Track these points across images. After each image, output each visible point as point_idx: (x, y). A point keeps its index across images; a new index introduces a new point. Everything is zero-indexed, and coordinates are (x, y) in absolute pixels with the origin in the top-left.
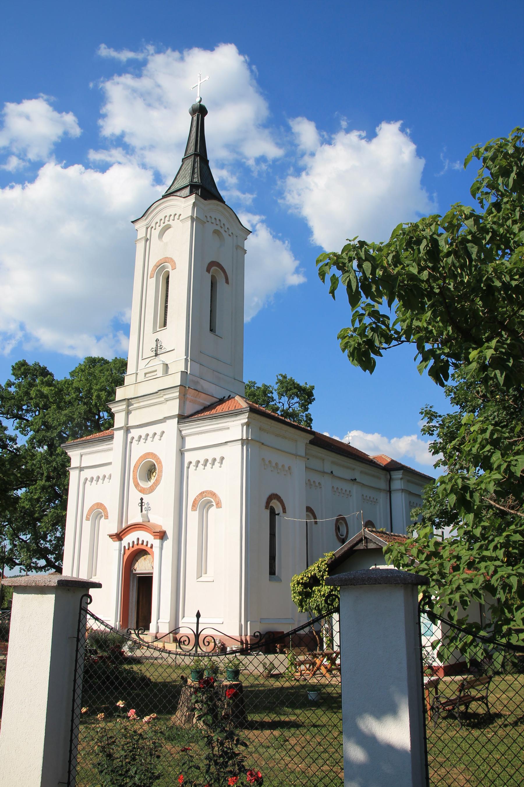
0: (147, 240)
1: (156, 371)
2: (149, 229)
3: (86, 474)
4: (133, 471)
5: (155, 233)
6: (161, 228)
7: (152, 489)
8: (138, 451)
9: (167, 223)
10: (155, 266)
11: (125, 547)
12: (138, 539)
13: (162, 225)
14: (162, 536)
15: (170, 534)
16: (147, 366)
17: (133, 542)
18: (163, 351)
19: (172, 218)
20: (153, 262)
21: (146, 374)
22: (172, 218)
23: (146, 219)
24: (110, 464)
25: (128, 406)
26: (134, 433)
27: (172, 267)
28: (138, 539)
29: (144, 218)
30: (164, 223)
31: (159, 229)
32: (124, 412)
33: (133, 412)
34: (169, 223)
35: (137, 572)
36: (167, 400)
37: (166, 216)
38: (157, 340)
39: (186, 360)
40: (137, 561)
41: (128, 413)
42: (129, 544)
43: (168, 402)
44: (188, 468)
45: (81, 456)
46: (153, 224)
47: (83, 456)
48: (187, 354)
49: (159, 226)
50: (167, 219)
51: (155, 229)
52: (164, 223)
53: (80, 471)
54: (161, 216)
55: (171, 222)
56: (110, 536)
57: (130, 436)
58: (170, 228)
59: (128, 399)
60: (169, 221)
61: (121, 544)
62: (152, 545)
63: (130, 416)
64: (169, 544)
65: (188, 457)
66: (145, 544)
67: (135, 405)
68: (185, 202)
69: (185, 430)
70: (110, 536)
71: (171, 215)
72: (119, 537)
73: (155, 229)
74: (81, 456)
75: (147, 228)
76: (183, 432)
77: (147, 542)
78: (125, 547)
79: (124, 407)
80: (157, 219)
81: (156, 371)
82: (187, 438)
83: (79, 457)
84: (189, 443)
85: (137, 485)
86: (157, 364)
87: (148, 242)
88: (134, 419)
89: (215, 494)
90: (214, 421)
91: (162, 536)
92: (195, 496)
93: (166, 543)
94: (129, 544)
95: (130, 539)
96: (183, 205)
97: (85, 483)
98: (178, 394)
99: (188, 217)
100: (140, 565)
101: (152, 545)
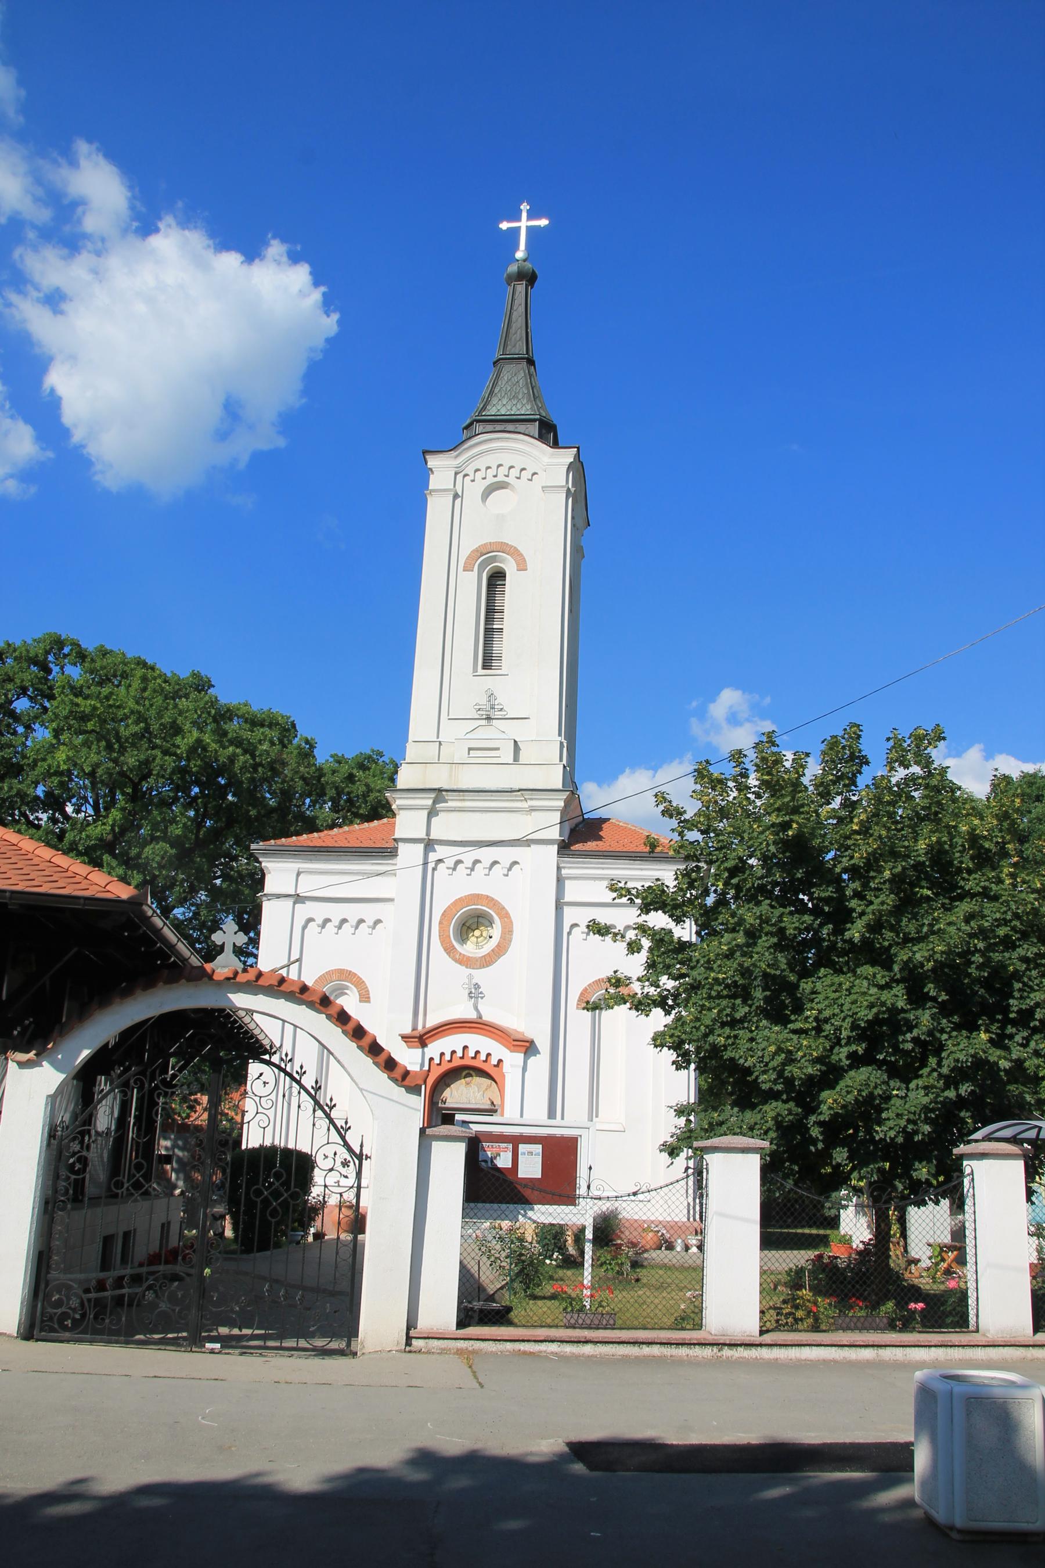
0: (456, 496)
1: (498, 749)
2: (460, 477)
3: (304, 911)
4: (440, 923)
5: (473, 490)
6: (487, 482)
7: (487, 961)
8: (451, 888)
9: (501, 478)
10: (476, 550)
11: (431, 1059)
12: (465, 1048)
13: (490, 480)
14: (529, 1048)
15: (543, 1044)
16: (468, 736)
17: (453, 1052)
18: (498, 715)
19: (514, 472)
20: (468, 545)
21: (470, 749)
22: (514, 472)
23: (456, 457)
24: (391, 900)
25: (435, 802)
26: (441, 851)
27: (518, 565)
28: (465, 1048)
29: (454, 454)
30: (495, 476)
31: (481, 486)
32: (425, 813)
33: (441, 814)
34: (506, 479)
35: (447, 1105)
36: (533, 809)
37: (500, 466)
39: (561, 743)
40: (449, 1086)
41: (432, 813)
42: (442, 1054)
43: (533, 813)
44: (569, 933)
45: (298, 874)
46: (470, 470)
47: (302, 876)
48: (560, 735)
49: (484, 478)
50: (502, 471)
51: (473, 481)
52: (495, 476)
53: (295, 903)
54: (492, 460)
55: (511, 480)
57: (433, 857)
58: (503, 488)
59: (440, 790)
60: (507, 476)
61: (423, 1054)
63: (434, 820)
64: (540, 1064)
65: (570, 915)
66: (483, 1057)
67: (450, 804)
68: (552, 455)
69: (570, 868)
70: (405, 1038)
73: (473, 481)
74: (298, 874)
75: (456, 474)
76: (564, 872)
77: (489, 1055)
78: (431, 1059)
79: (430, 802)
80: (481, 463)
81: (498, 749)
82: (567, 882)
83: (295, 875)
84: (573, 892)
85: (450, 950)
86: (487, 734)
87: (458, 501)
88: (444, 827)
90: (637, 865)
91: (529, 1048)
92: (586, 985)
93: (532, 1060)
94: (442, 1054)
96: (546, 460)
97: (304, 927)
98: (562, 804)
99: (563, 487)
100: (455, 1093)
101: (500, 1061)
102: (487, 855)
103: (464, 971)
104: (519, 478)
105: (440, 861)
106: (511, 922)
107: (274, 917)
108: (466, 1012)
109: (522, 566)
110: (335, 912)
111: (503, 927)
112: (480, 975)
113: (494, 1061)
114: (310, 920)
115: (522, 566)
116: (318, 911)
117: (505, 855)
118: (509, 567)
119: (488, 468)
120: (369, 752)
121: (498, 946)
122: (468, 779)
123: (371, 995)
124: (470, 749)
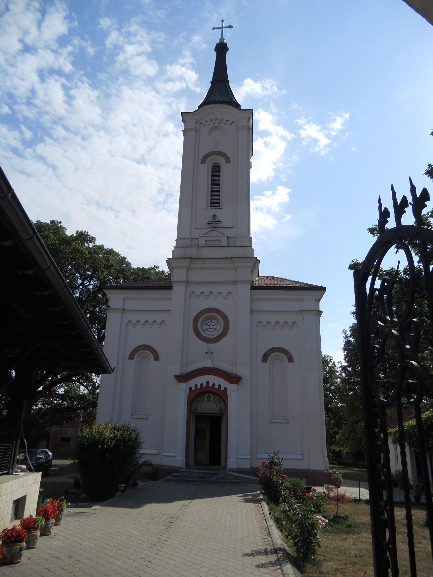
0: (196, 131)
2: (198, 124)
6: (211, 126)
7: (217, 339)
9: (217, 124)
16: (205, 235)
38: (214, 216)
45: (124, 299)
46: (203, 121)
52: (214, 124)
55: (222, 125)
56: (177, 377)
62: (225, 389)
66: (217, 387)
71: (222, 120)
72: (183, 378)
89: (286, 350)
95: (200, 381)
102: (216, 289)
103: (205, 345)
104: (225, 124)
105: (193, 292)
106: (228, 321)
107: (112, 320)
108: (208, 364)
109: (228, 160)
110: (142, 318)
111: (225, 324)
112: (214, 346)
113: (222, 389)
114: (130, 321)
115: (228, 160)
116: (134, 317)
117: (225, 289)
118: (222, 161)
119: (211, 120)
120: (153, 266)
121: (222, 332)
122: (207, 253)
123: (160, 357)
124: (206, 241)
